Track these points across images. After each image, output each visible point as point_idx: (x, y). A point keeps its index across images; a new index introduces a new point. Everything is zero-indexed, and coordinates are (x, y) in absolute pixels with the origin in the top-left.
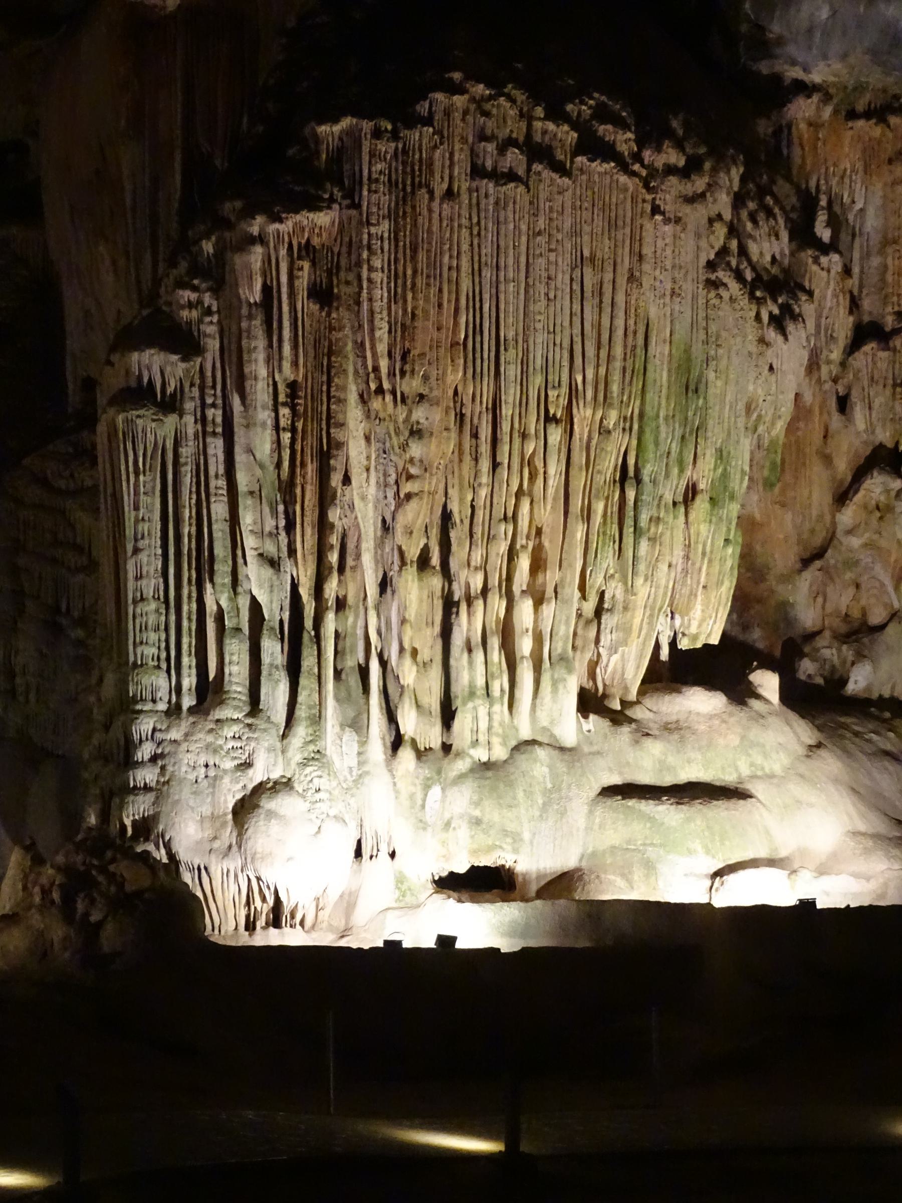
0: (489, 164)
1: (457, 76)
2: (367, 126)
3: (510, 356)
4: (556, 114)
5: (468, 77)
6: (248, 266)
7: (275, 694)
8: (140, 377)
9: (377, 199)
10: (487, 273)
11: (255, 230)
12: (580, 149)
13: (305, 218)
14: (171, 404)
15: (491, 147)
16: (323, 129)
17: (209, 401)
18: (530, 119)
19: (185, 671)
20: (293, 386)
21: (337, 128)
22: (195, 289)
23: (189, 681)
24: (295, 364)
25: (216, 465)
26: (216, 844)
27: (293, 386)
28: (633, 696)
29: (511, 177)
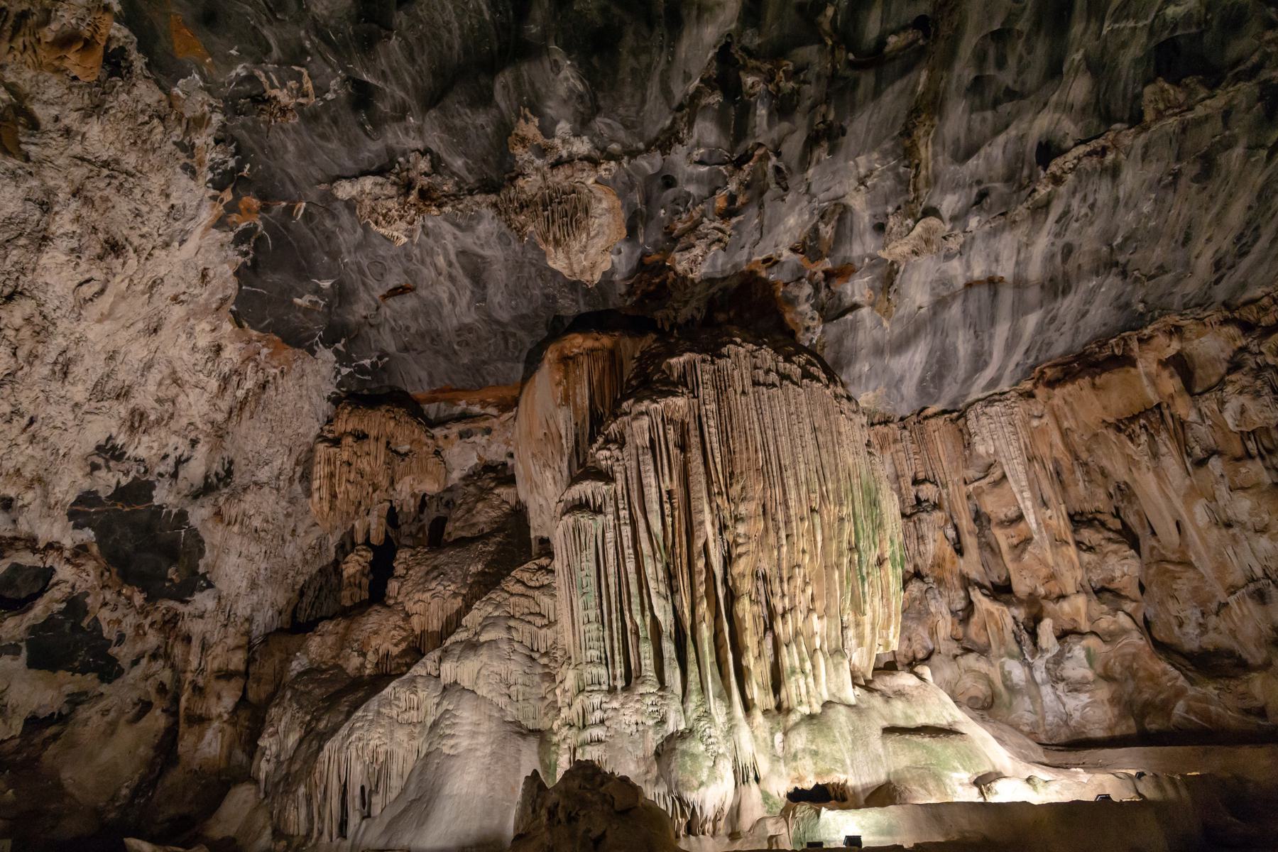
0: (761, 380)
1: (738, 340)
2: (698, 357)
3: (789, 473)
4: (788, 359)
5: (744, 340)
6: (641, 427)
7: (673, 676)
8: (580, 498)
9: (707, 392)
10: (770, 432)
11: (643, 409)
12: (803, 377)
13: (671, 400)
14: (599, 511)
15: (761, 372)
16: (673, 361)
17: (621, 506)
18: (777, 363)
19: (617, 665)
20: (669, 493)
21: (682, 359)
22: (609, 449)
23: (620, 670)
24: (671, 479)
25: (627, 542)
26: (649, 777)
27: (669, 493)
28: (870, 676)
29: (774, 385)
